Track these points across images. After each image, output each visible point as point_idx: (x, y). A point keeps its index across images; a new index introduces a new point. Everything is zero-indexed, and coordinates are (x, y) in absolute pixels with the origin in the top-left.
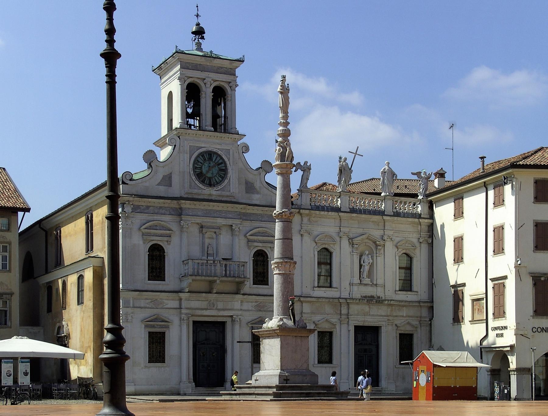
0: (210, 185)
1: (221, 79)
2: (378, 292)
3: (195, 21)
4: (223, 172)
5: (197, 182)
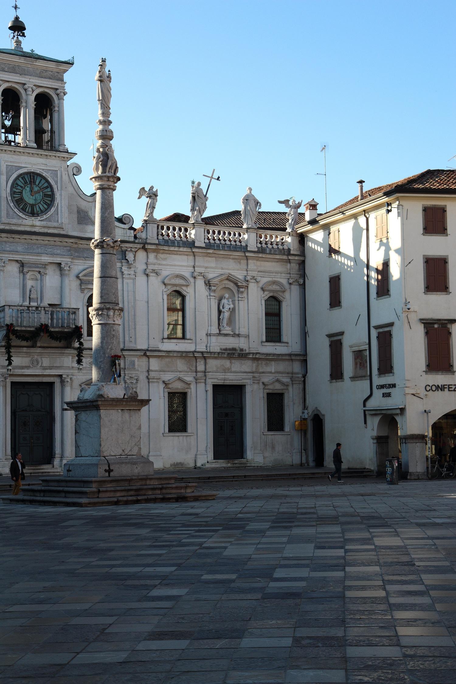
0: (33, 214)
4: (49, 198)
5: (16, 210)
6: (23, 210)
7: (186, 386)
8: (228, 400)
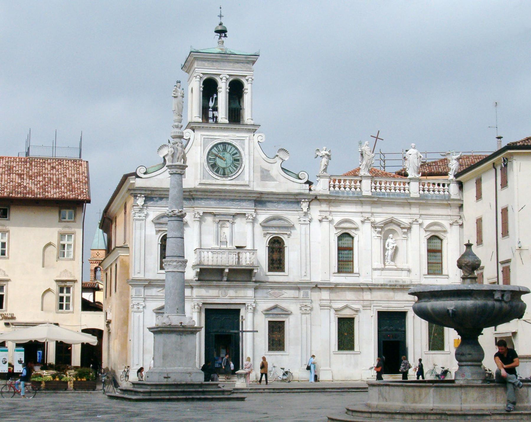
0: (224, 175)
1: (237, 71)
2: (403, 278)
3: (218, 21)
4: (237, 161)
5: (211, 173)
6: (217, 172)
7: (355, 313)
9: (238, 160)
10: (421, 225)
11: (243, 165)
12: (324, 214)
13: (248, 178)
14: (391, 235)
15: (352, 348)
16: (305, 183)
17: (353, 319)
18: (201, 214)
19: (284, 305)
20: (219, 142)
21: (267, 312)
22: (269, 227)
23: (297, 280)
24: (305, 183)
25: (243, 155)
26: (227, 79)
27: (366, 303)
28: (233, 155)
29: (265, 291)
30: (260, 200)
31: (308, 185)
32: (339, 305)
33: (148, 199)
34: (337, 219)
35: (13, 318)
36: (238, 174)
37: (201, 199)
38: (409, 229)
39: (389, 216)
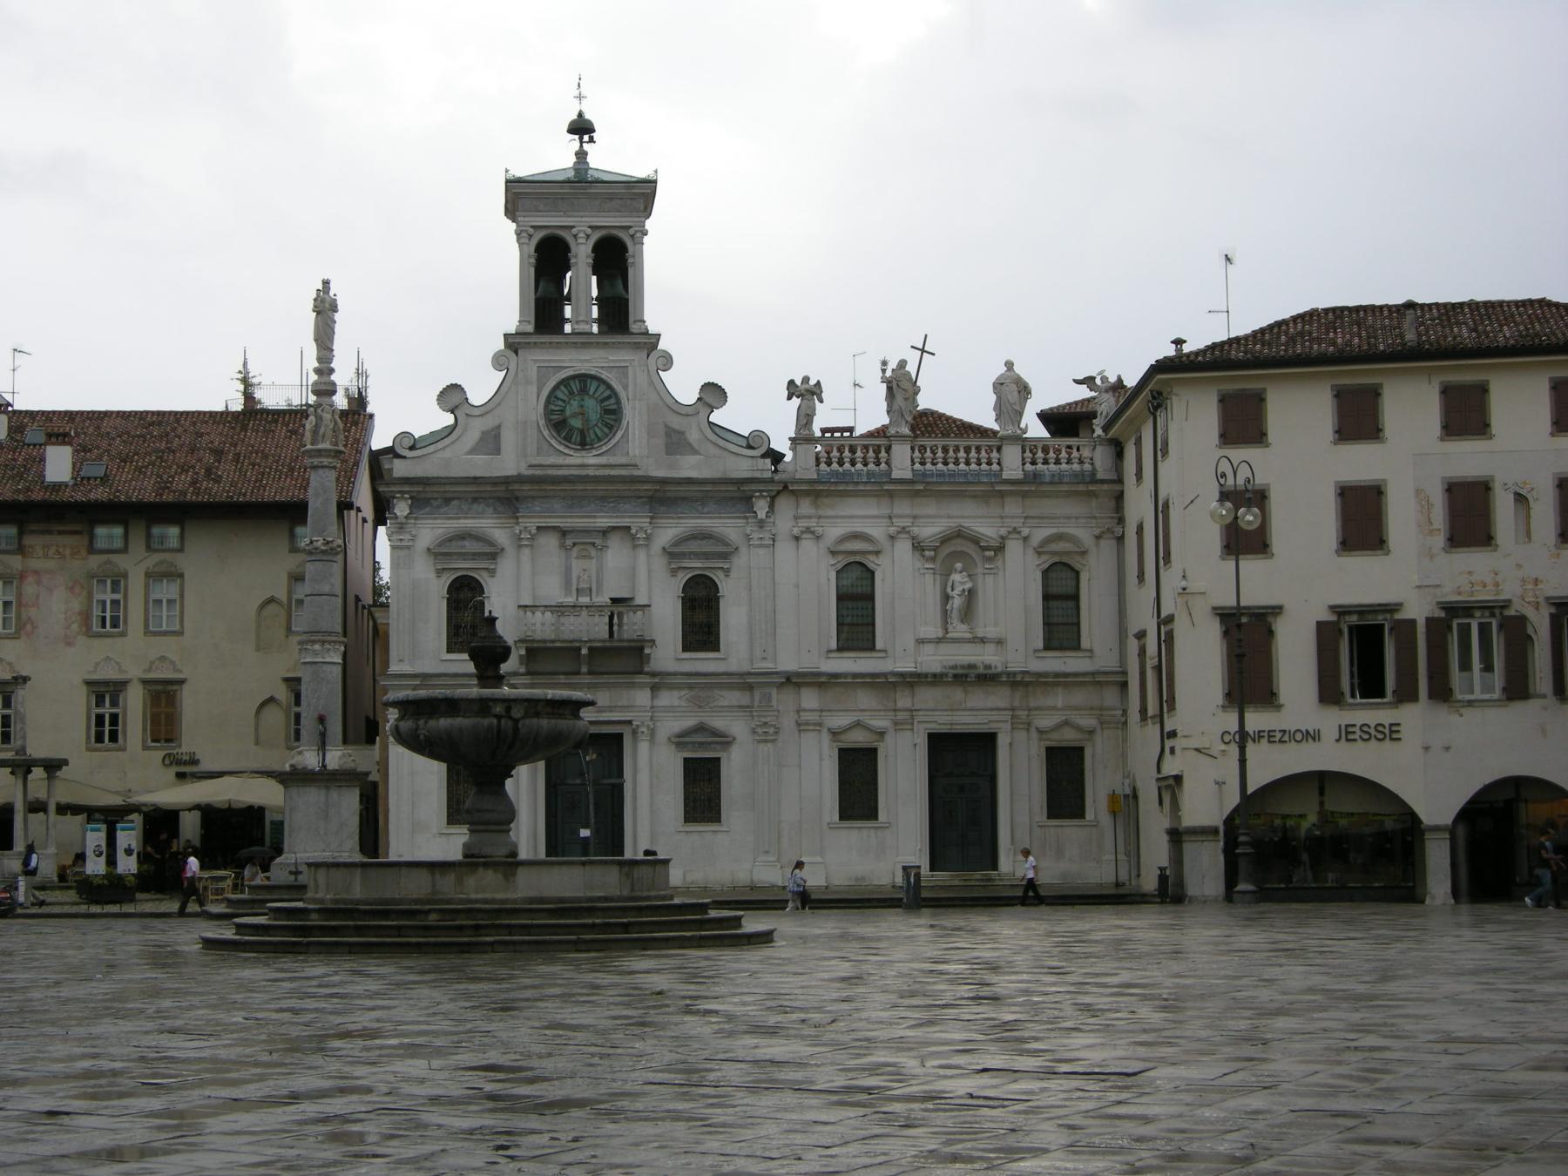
0: (584, 444)
2: (987, 657)
4: (612, 414)
6: (568, 439)
8: (961, 764)
9: (613, 412)
10: (1026, 539)
11: (624, 423)
12: (803, 524)
13: (635, 447)
14: (959, 566)
15: (871, 813)
16: (763, 456)
17: (875, 750)
18: (534, 531)
19: (718, 723)
20: (570, 373)
21: (680, 740)
22: (682, 555)
23: (746, 668)
24: (763, 456)
25: (624, 401)
26: (588, 236)
27: (901, 716)
28: (602, 401)
29: (676, 693)
30: (662, 496)
31: (768, 461)
32: (840, 721)
33: (418, 503)
34: (834, 532)
35: (195, 762)
36: (613, 441)
37: (533, 498)
38: (1000, 549)
39: (953, 523)
